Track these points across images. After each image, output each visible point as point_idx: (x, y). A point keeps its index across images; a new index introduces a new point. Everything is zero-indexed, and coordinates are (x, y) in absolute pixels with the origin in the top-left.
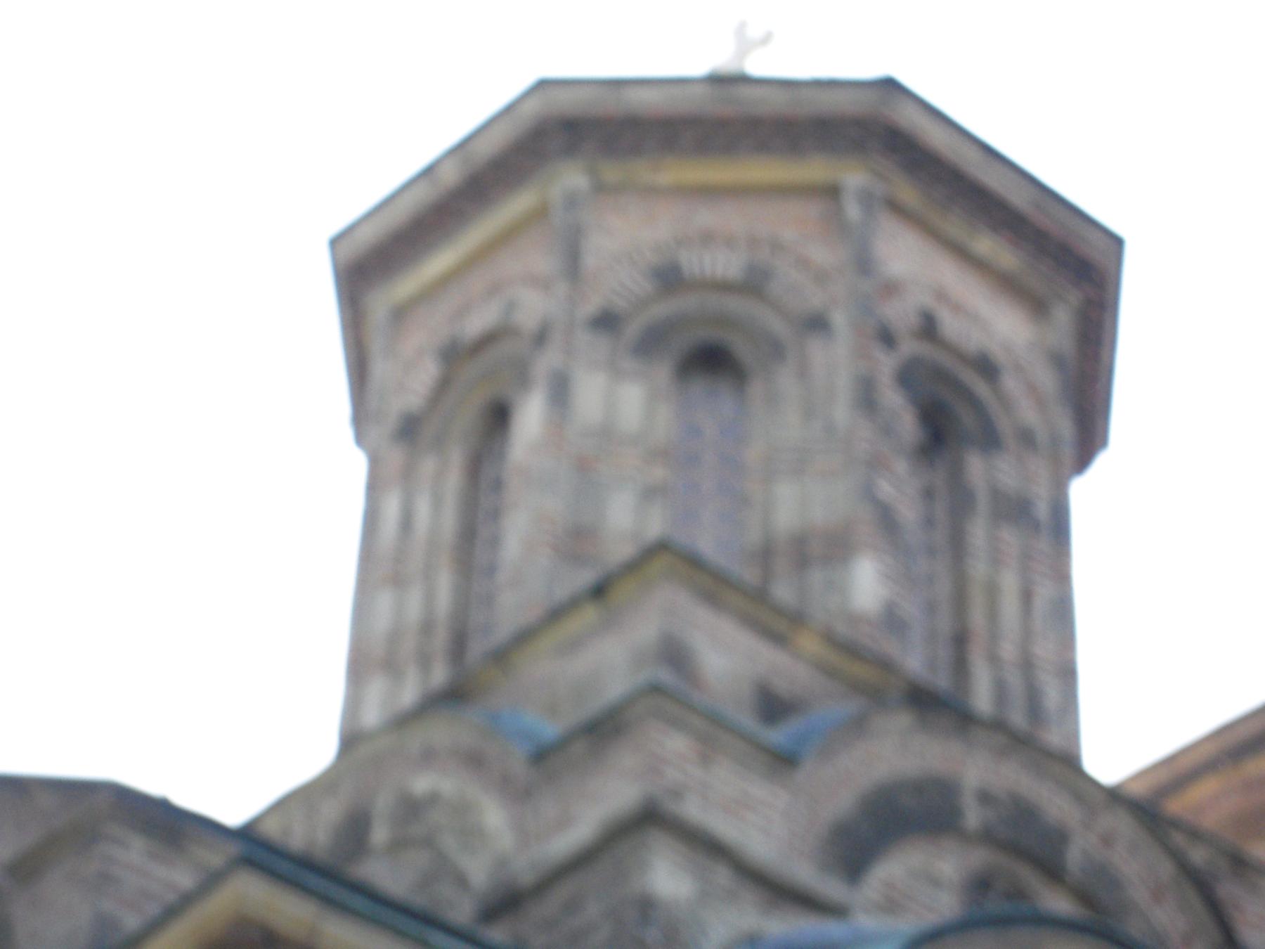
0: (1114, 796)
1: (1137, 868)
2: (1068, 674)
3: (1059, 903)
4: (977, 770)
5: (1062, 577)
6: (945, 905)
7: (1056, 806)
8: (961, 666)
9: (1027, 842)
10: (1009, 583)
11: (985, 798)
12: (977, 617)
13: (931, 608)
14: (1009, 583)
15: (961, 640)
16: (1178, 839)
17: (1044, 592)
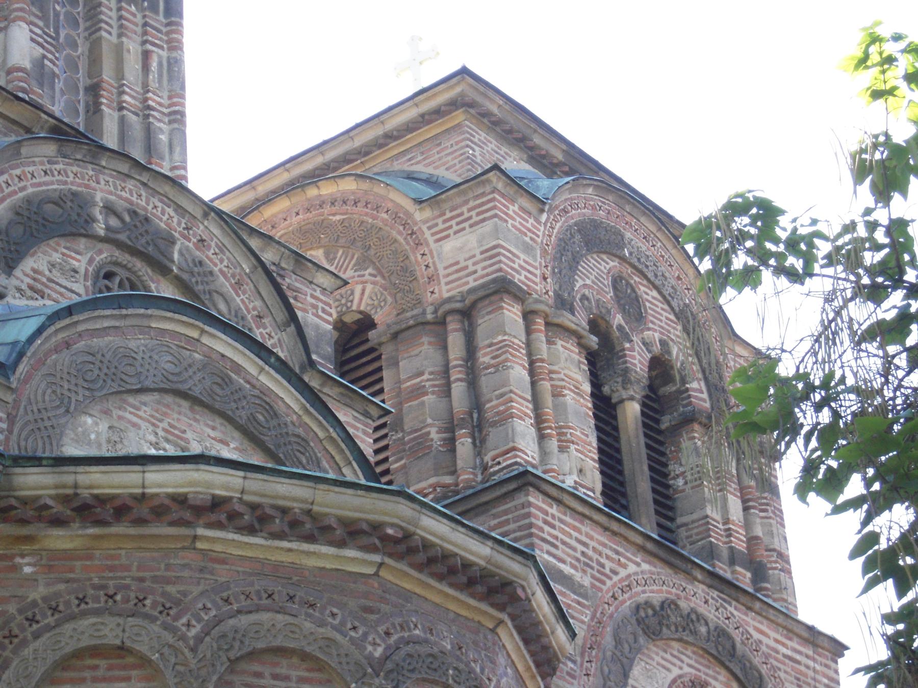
0: (209, 209)
1: (224, 265)
2: (177, 118)
3: (167, 291)
4: (105, 189)
5: (175, 45)
6: (81, 290)
7: (164, 217)
8: (94, 109)
9: (142, 243)
10: (132, 47)
11: (109, 209)
12: (107, 75)
13: (72, 65)
14: (132, 47)
15: (94, 90)
16: (254, 243)
17: (159, 55)
